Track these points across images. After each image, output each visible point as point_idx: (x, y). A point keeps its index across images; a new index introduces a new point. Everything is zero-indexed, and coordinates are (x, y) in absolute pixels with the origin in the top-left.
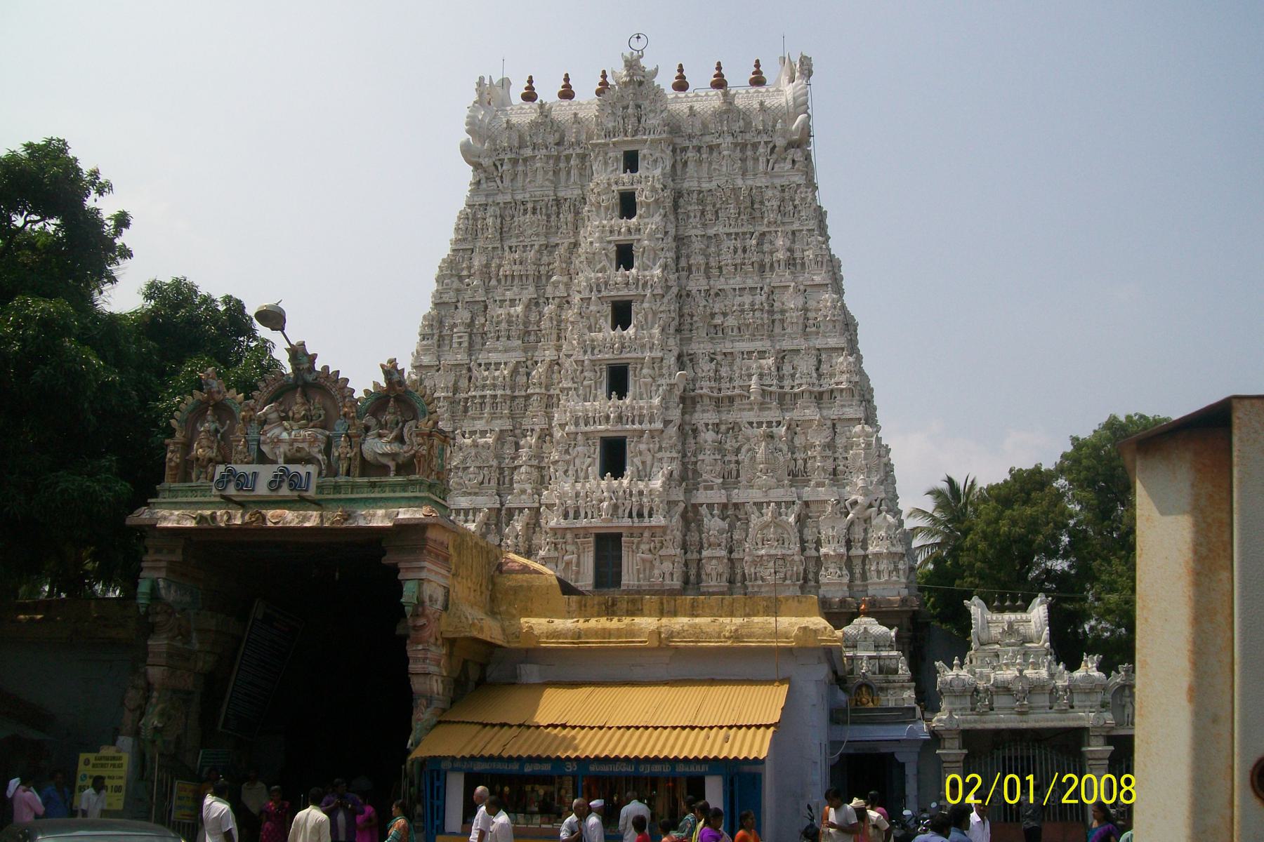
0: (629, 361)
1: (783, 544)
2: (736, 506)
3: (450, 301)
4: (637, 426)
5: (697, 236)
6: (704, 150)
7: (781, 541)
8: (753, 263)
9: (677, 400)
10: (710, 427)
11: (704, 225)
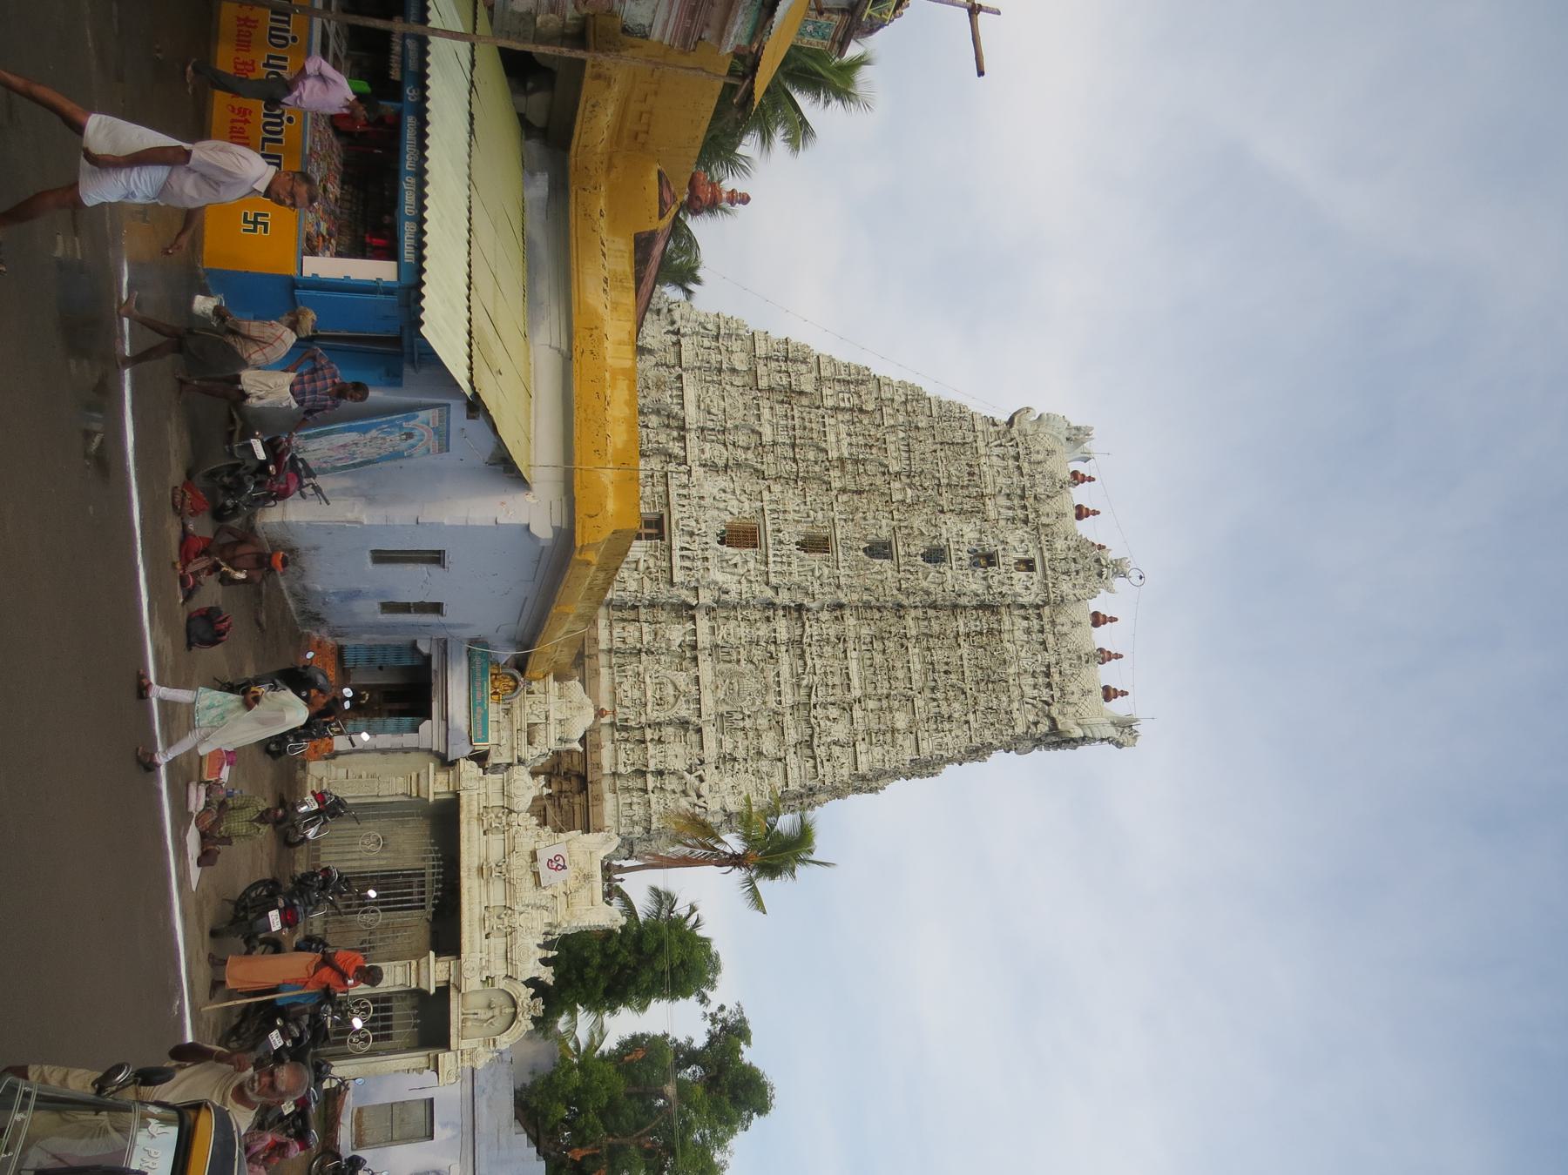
0: (835, 554)
1: (658, 705)
2: (695, 659)
3: (882, 393)
4: (771, 559)
5: (957, 627)
7: (660, 702)
8: (935, 681)
9: (799, 601)
10: (773, 635)
11: (968, 635)
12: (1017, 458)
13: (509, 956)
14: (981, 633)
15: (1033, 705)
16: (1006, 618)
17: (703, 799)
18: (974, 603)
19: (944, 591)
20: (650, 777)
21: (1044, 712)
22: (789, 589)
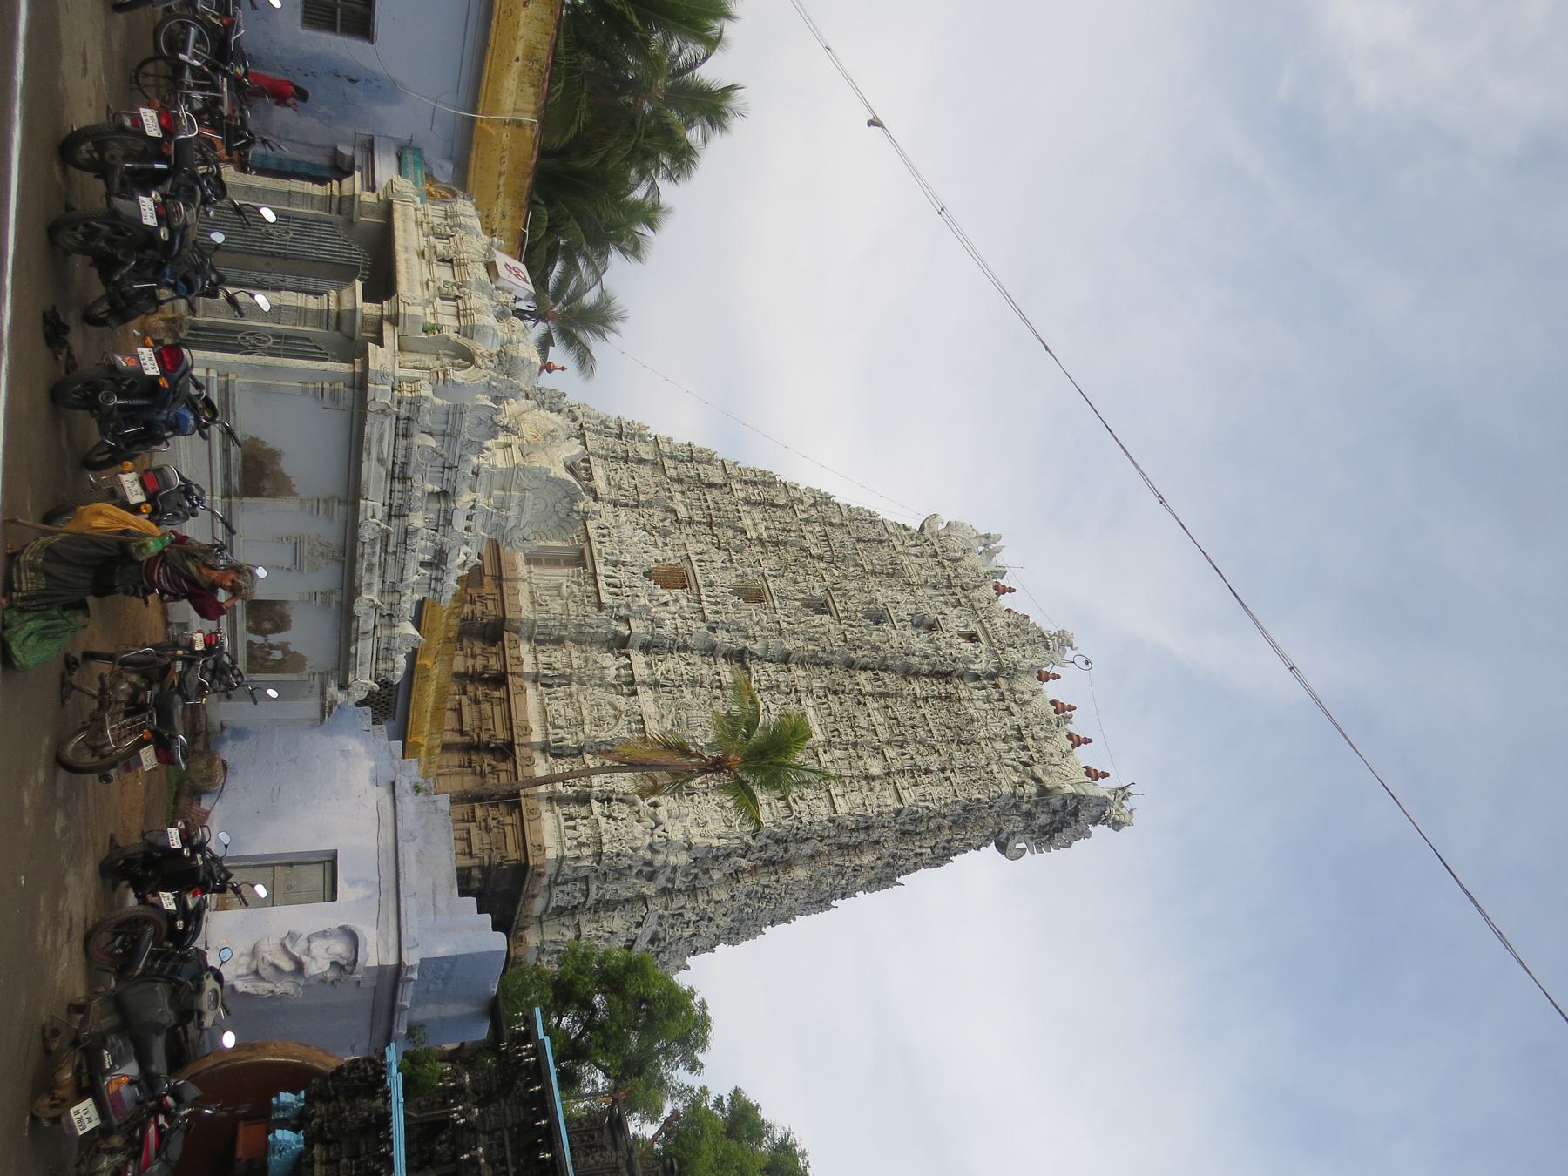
2: (634, 693)
4: (704, 597)
6: (1002, 703)
7: (599, 722)
8: (903, 734)
10: (717, 677)
12: (935, 555)
13: (461, 308)
14: (939, 697)
15: (1013, 766)
16: (961, 686)
17: (662, 827)
18: (925, 668)
19: (892, 647)
20: (595, 805)
21: (1027, 774)
22: (728, 631)
